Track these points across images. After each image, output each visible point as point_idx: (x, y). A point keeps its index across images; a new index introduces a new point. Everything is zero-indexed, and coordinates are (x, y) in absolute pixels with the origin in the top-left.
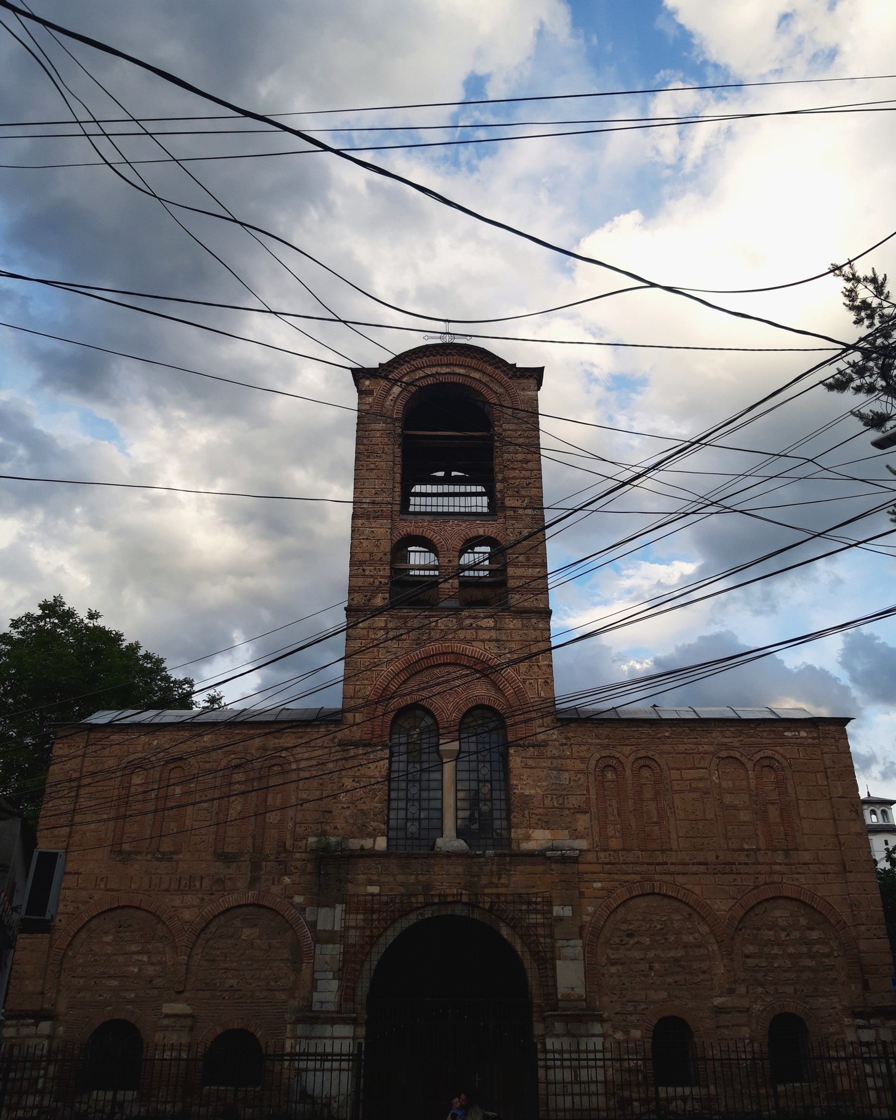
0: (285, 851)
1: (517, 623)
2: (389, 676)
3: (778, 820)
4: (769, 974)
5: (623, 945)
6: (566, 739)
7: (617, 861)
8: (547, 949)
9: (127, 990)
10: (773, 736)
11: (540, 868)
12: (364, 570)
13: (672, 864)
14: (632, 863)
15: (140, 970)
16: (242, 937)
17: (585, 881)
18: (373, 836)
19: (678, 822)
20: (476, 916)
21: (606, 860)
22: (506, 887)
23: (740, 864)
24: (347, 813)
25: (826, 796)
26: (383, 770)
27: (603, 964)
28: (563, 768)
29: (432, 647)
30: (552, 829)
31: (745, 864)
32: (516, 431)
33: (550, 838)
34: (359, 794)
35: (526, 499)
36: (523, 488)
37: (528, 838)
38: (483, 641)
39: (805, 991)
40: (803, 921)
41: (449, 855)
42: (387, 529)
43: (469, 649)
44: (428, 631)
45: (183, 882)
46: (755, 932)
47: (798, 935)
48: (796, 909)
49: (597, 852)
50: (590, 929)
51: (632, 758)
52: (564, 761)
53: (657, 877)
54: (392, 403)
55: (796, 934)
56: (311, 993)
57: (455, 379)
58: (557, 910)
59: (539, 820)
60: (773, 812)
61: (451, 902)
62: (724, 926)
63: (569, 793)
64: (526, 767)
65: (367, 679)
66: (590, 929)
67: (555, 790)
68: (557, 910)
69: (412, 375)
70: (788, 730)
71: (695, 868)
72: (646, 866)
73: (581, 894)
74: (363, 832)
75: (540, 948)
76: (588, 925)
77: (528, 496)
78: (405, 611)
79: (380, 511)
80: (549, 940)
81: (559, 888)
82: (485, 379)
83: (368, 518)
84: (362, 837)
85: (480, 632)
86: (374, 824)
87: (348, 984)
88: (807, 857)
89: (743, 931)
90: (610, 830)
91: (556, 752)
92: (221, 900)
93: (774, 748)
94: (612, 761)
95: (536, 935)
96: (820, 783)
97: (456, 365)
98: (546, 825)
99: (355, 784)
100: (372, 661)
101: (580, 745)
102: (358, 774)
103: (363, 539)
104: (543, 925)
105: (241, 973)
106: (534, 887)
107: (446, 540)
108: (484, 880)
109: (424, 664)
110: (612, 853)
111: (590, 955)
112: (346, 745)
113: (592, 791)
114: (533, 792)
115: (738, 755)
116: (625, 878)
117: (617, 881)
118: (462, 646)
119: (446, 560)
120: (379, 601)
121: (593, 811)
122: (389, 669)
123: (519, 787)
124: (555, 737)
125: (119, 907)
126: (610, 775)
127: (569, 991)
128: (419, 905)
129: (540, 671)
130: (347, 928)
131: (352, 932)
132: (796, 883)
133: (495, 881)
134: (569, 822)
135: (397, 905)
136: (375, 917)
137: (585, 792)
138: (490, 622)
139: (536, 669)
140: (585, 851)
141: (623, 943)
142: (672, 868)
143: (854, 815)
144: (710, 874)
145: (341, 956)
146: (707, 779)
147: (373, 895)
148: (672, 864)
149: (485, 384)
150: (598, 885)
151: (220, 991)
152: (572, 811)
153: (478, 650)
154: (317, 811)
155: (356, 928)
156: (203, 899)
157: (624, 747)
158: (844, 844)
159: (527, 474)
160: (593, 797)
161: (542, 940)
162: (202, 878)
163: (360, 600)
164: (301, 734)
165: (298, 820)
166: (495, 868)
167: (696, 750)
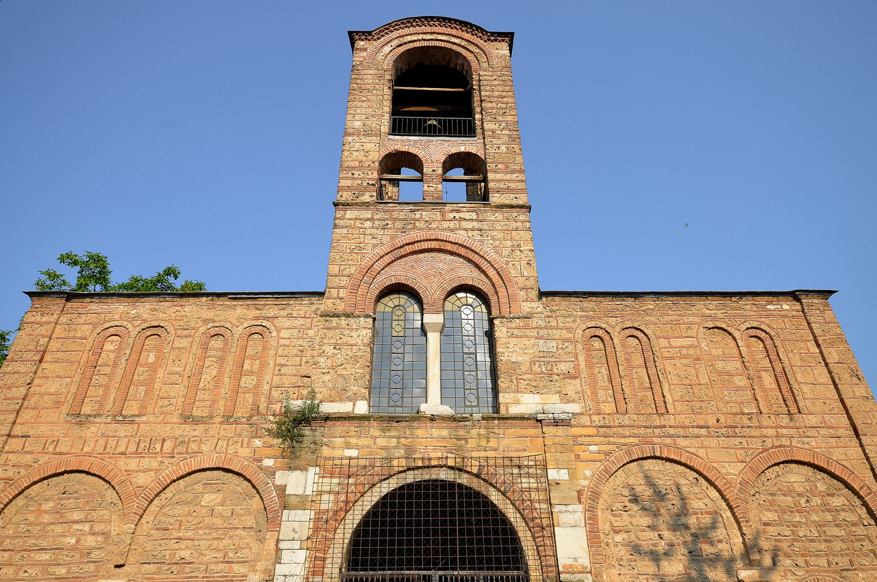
0: (258, 413)
1: (499, 216)
2: (374, 258)
3: (774, 386)
4: (795, 544)
5: (626, 511)
6: (551, 312)
7: (612, 424)
8: (542, 516)
9: (59, 564)
10: (755, 309)
11: (532, 431)
12: (353, 174)
13: (670, 427)
14: (629, 426)
15: (78, 541)
16: (202, 504)
17: (580, 445)
18: (353, 399)
19: (672, 387)
20: (464, 480)
21: (602, 423)
22: (495, 450)
23: (743, 427)
24: (327, 378)
25: (820, 363)
26: (365, 339)
27: (606, 532)
28: (550, 338)
29: (414, 235)
30: (542, 394)
31: (749, 427)
32: (492, 76)
33: (540, 402)
34: (340, 360)
35: (503, 123)
36: (500, 115)
37: (517, 402)
38: (466, 230)
39: (840, 564)
40: (821, 487)
41: (433, 418)
42: (376, 144)
43: (453, 237)
44: (412, 222)
45: (142, 445)
46: (770, 498)
47: (819, 502)
48: (810, 474)
49: (590, 415)
50: (589, 493)
51: (618, 329)
52: (550, 331)
53: (656, 440)
54: (383, 57)
55: (816, 501)
56: (274, 565)
57: (438, 44)
58: (553, 474)
59: (527, 384)
60: (768, 380)
61: (433, 467)
62: (736, 490)
63: (556, 360)
64: (512, 336)
65: (352, 260)
66: (589, 493)
67: (543, 357)
68: (553, 474)
69: (401, 39)
70: (771, 303)
71: (696, 431)
72: (643, 429)
73: (578, 457)
74: (341, 395)
75: (535, 514)
76: (586, 489)
77: (505, 121)
78: (390, 205)
79: (370, 131)
80: (544, 506)
81: (554, 451)
82: (463, 43)
83: (358, 135)
84: (341, 400)
85: (463, 223)
86: (355, 389)
87: (318, 554)
88: (813, 420)
89: (757, 495)
90: (601, 394)
91: (542, 324)
92: (181, 464)
93: (759, 320)
94: (598, 331)
95: (530, 500)
96: (812, 351)
97: (438, 34)
98: (536, 390)
99: (336, 351)
100: (357, 245)
101: (566, 317)
102: (340, 342)
103: (353, 151)
104: (537, 490)
105: (196, 543)
106: (525, 450)
107: (431, 155)
108: (472, 444)
109: (409, 249)
110: (607, 417)
111: (591, 522)
112: (328, 315)
113: (581, 358)
114: (520, 359)
115: (724, 326)
116: (622, 441)
117: (614, 444)
118: (446, 234)
119: (431, 170)
120: (366, 198)
121: (583, 376)
122: (374, 252)
123: (506, 354)
124: (539, 310)
125: (66, 472)
126: (597, 344)
127: (571, 562)
128: (402, 469)
129: (522, 254)
130: (320, 493)
131: (325, 497)
132: (806, 446)
133: (484, 443)
134: (560, 387)
135: (376, 469)
136: (351, 481)
137: (574, 359)
138: (474, 216)
139: (518, 253)
140: (577, 414)
141: (626, 509)
142: (672, 431)
143: (855, 380)
144: (712, 437)
145: (312, 523)
146: (696, 346)
147: (350, 458)
148: (670, 427)
149: (464, 47)
150: (594, 448)
151: (169, 564)
152: (562, 377)
153: (461, 237)
154: (296, 376)
155: (329, 492)
156: (162, 462)
157: (610, 319)
158: (851, 407)
159: (504, 106)
160: (582, 363)
161: (537, 505)
162: (164, 441)
163: (348, 197)
164: (284, 306)
165: (274, 384)
166: (482, 431)
167: (681, 321)
